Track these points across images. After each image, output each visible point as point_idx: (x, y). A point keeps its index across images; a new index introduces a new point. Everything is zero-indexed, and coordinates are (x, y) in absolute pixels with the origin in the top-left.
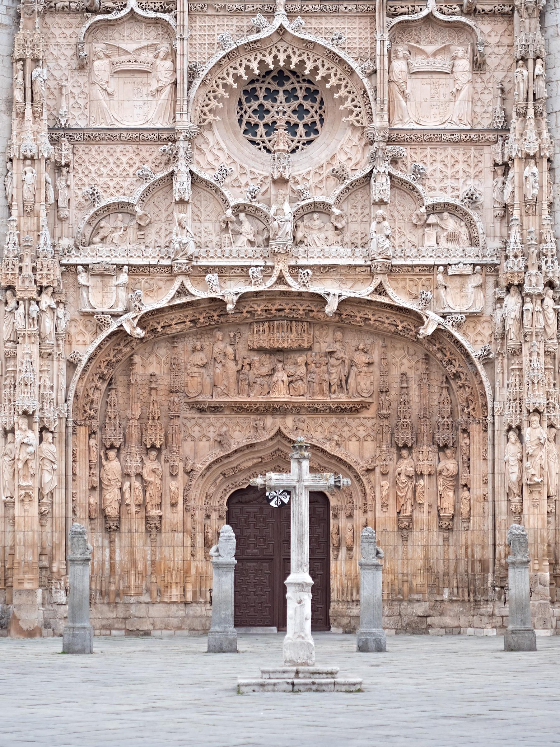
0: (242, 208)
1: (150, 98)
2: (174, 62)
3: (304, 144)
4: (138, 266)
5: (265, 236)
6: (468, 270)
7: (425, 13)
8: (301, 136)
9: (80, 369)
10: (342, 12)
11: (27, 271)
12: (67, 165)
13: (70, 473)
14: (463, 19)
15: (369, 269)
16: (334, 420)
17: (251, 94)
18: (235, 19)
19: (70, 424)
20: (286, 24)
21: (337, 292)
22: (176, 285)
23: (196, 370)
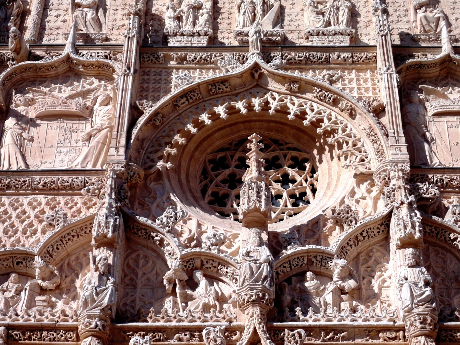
0: (198, 263)
1: (81, 143)
3: (291, 216)
4: (24, 329)
8: (286, 206)
15: (401, 333)
18: (197, 73)
20: (261, 63)
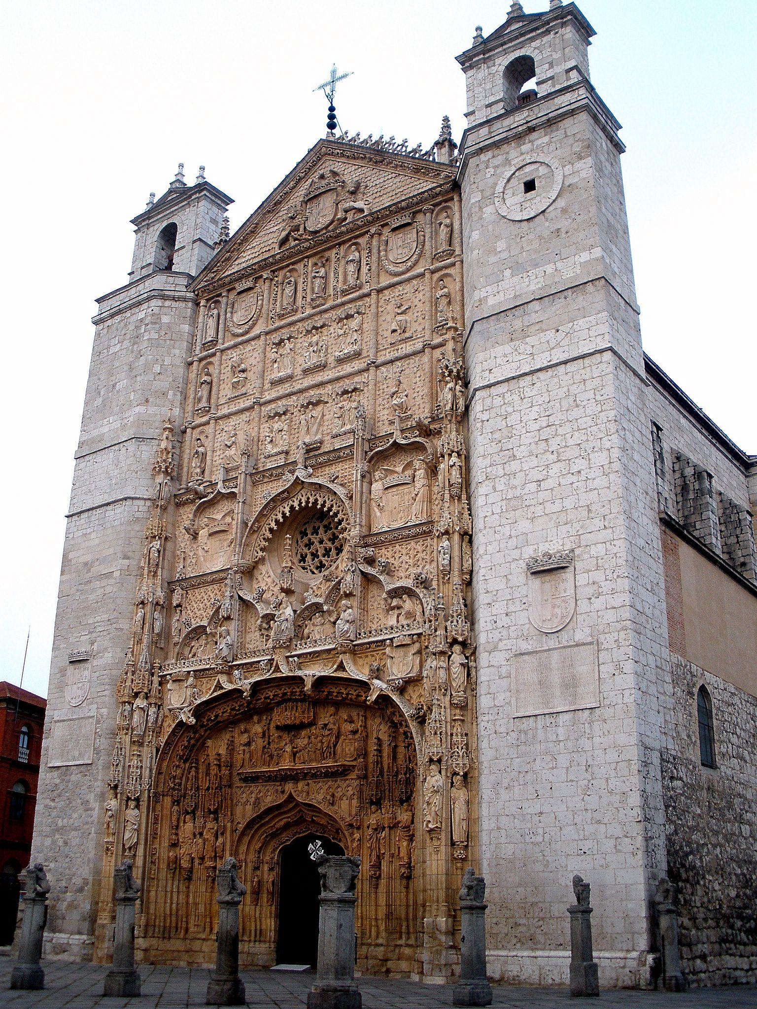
6: (407, 641)
7: (391, 441)
10: (343, 457)
11: (128, 683)
12: (179, 605)
14: (417, 439)
16: (329, 783)
21: (311, 672)
23: (242, 748)
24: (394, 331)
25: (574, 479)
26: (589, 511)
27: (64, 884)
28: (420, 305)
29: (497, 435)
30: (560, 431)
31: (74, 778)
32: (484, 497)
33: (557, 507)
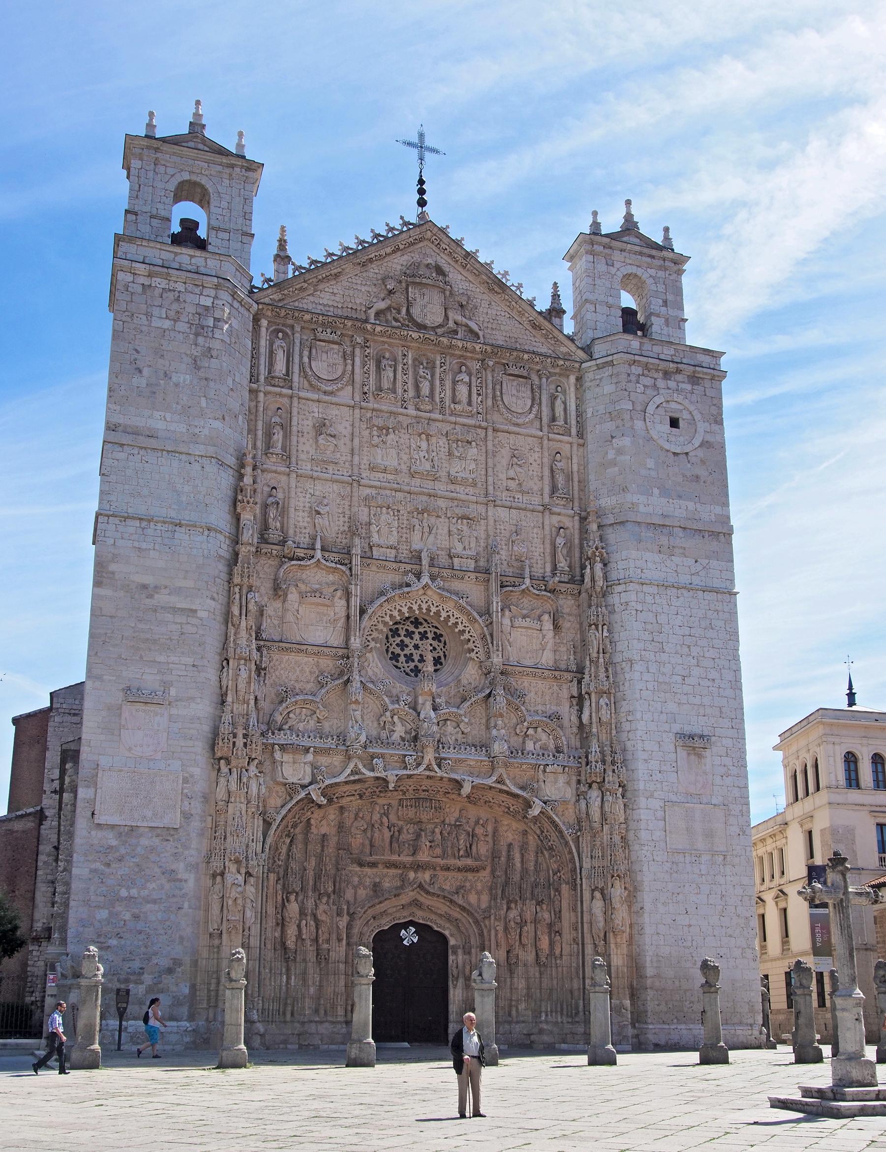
1: (329, 625)
2: (348, 601)
5: (413, 734)
9: (274, 827)
12: (265, 669)
13: (264, 911)
17: (395, 633)
19: (266, 871)
22: (351, 766)
24: (513, 479)
25: (710, 683)
26: (721, 712)
27: (136, 965)
28: (534, 463)
29: (649, 627)
30: (699, 643)
31: (144, 842)
32: (639, 674)
33: (697, 701)
